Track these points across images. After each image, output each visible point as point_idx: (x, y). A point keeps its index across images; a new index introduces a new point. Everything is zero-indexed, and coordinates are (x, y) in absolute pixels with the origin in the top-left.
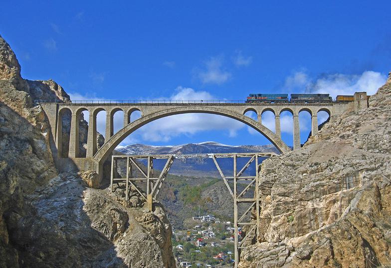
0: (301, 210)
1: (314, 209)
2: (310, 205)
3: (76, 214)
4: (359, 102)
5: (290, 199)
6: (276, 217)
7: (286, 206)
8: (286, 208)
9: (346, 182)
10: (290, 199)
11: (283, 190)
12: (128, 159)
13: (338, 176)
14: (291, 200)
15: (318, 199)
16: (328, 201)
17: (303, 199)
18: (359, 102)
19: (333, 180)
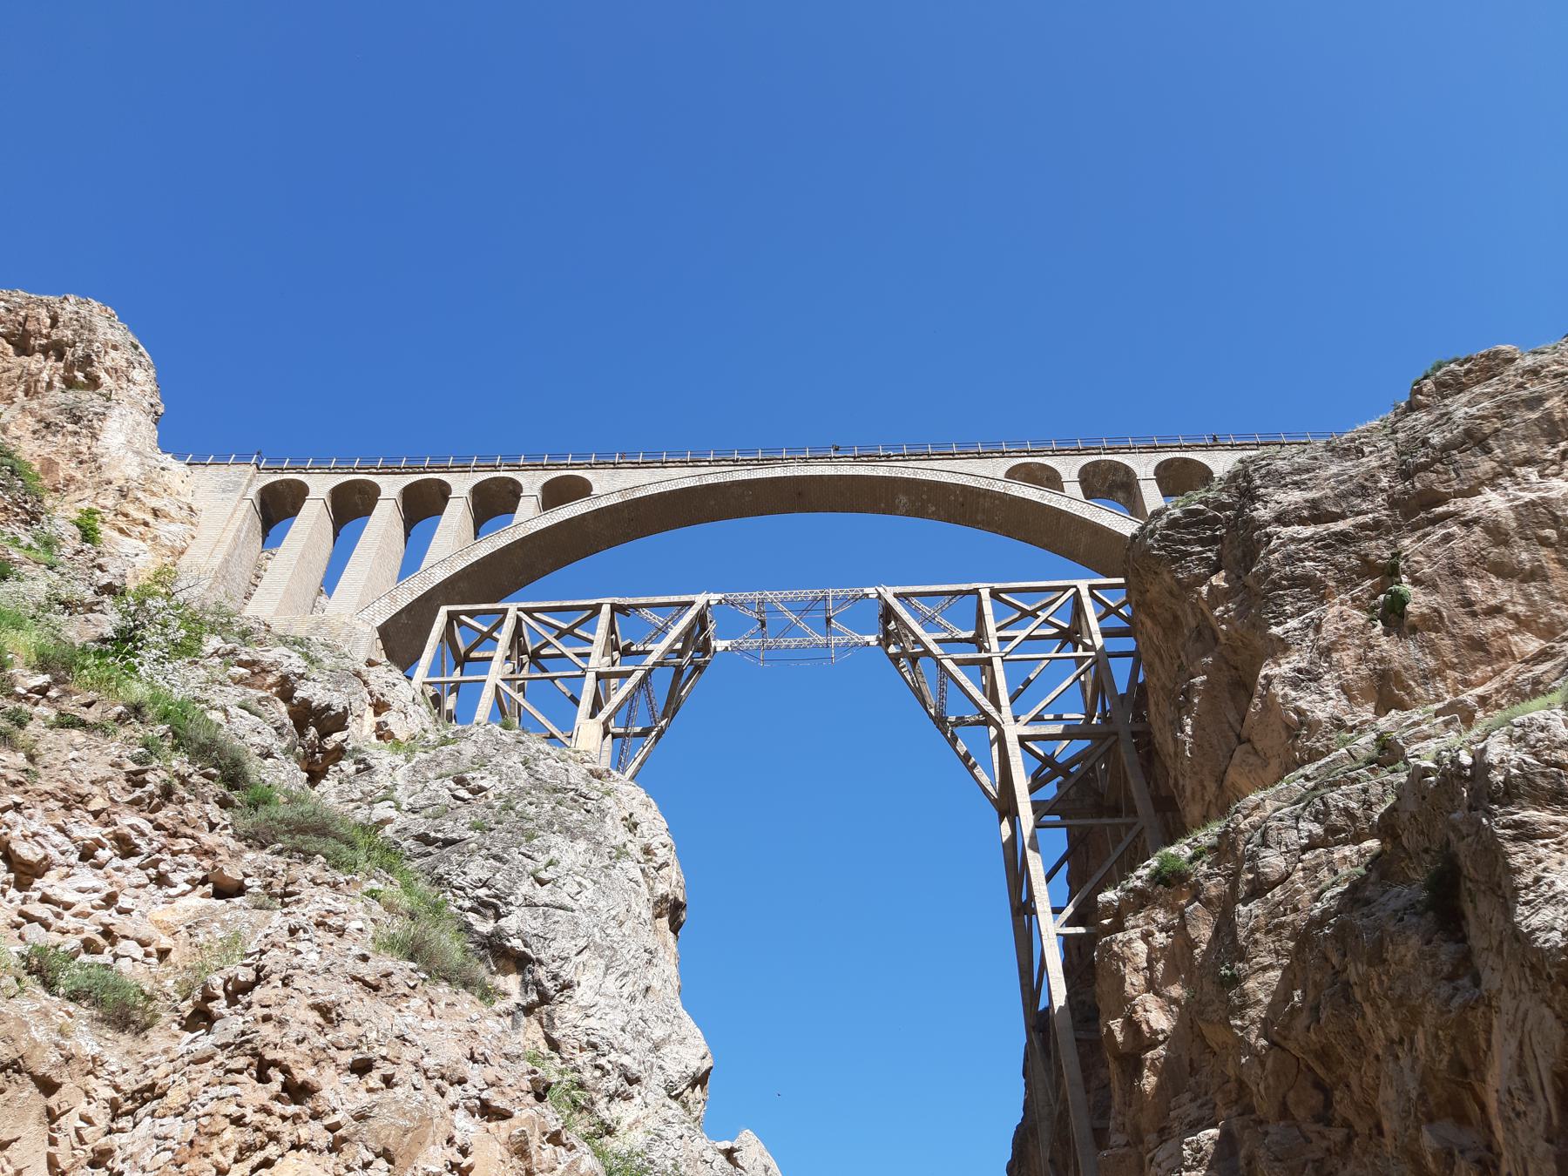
8: (1338, 567)
11: (1293, 497)
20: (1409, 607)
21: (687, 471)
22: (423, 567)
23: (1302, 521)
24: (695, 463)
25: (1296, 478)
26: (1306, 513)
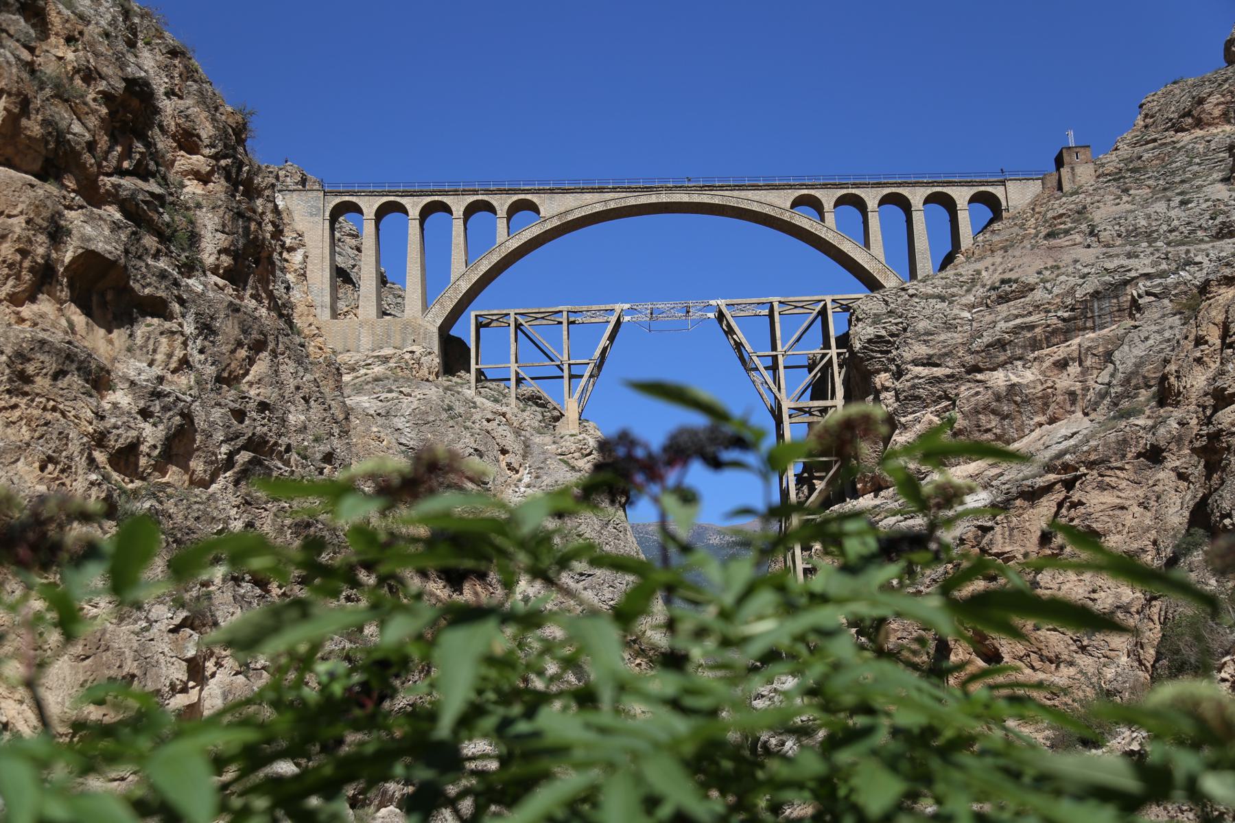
0: (977, 393)
1: (1013, 385)
2: (999, 379)
3: (400, 425)
4: (1073, 169)
5: (939, 372)
6: (910, 417)
7: (934, 389)
8: (933, 394)
9: (1092, 312)
10: (939, 372)
11: (922, 350)
12: (512, 319)
13: (1069, 301)
14: (948, 371)
15: (1019, 363)
16: (1047, 364)
17: (981, 364)
18: (1073, 169)
19: (1055, 312)
20: (955, 425)
21: (596, 197)
22: (453, 279)
23: (924, 365)
24: (601, 190)
25: (925, 338)
26: (925, 361)
